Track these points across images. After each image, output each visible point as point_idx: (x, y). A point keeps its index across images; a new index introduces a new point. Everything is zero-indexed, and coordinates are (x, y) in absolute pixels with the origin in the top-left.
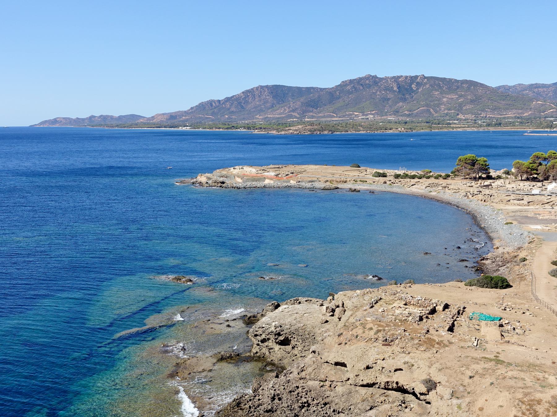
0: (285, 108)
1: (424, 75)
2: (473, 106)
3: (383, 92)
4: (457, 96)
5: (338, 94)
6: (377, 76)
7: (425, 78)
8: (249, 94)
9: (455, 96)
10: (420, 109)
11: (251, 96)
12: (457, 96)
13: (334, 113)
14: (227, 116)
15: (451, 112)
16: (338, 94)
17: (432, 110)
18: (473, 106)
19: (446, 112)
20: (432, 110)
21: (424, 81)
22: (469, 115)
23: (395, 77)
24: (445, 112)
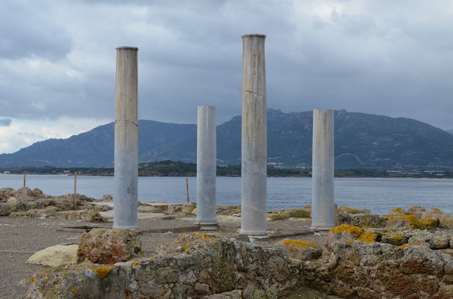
0: (154, 150)
1: (345, 110)
2: (415, 153)
3: (290, 132)
4: (392, 139)
5: (228, 133)
6: (282, 111)
7: (347, 114)
8: (104, 132)
9: (389, 139)
10: (342, 155)
11: (107, 134)
12: (392, 139)
13: (221, 159)
14: (70, 161)
15: (384, 160)
16: (228, 133)
17: (357, 157)
18: (415, 153)
19: (377, 159)
20: (357, 157)
21: (346, 119)
22: (411, 164)
23: (307, 112)
24: (376, 160)
